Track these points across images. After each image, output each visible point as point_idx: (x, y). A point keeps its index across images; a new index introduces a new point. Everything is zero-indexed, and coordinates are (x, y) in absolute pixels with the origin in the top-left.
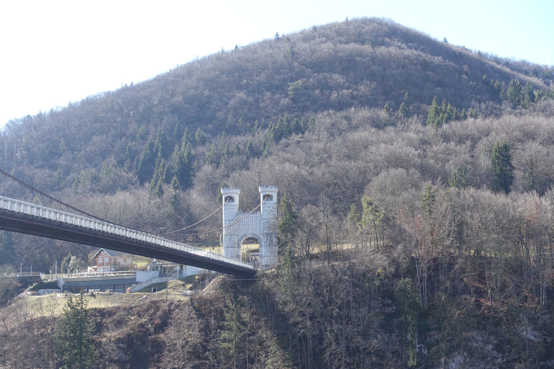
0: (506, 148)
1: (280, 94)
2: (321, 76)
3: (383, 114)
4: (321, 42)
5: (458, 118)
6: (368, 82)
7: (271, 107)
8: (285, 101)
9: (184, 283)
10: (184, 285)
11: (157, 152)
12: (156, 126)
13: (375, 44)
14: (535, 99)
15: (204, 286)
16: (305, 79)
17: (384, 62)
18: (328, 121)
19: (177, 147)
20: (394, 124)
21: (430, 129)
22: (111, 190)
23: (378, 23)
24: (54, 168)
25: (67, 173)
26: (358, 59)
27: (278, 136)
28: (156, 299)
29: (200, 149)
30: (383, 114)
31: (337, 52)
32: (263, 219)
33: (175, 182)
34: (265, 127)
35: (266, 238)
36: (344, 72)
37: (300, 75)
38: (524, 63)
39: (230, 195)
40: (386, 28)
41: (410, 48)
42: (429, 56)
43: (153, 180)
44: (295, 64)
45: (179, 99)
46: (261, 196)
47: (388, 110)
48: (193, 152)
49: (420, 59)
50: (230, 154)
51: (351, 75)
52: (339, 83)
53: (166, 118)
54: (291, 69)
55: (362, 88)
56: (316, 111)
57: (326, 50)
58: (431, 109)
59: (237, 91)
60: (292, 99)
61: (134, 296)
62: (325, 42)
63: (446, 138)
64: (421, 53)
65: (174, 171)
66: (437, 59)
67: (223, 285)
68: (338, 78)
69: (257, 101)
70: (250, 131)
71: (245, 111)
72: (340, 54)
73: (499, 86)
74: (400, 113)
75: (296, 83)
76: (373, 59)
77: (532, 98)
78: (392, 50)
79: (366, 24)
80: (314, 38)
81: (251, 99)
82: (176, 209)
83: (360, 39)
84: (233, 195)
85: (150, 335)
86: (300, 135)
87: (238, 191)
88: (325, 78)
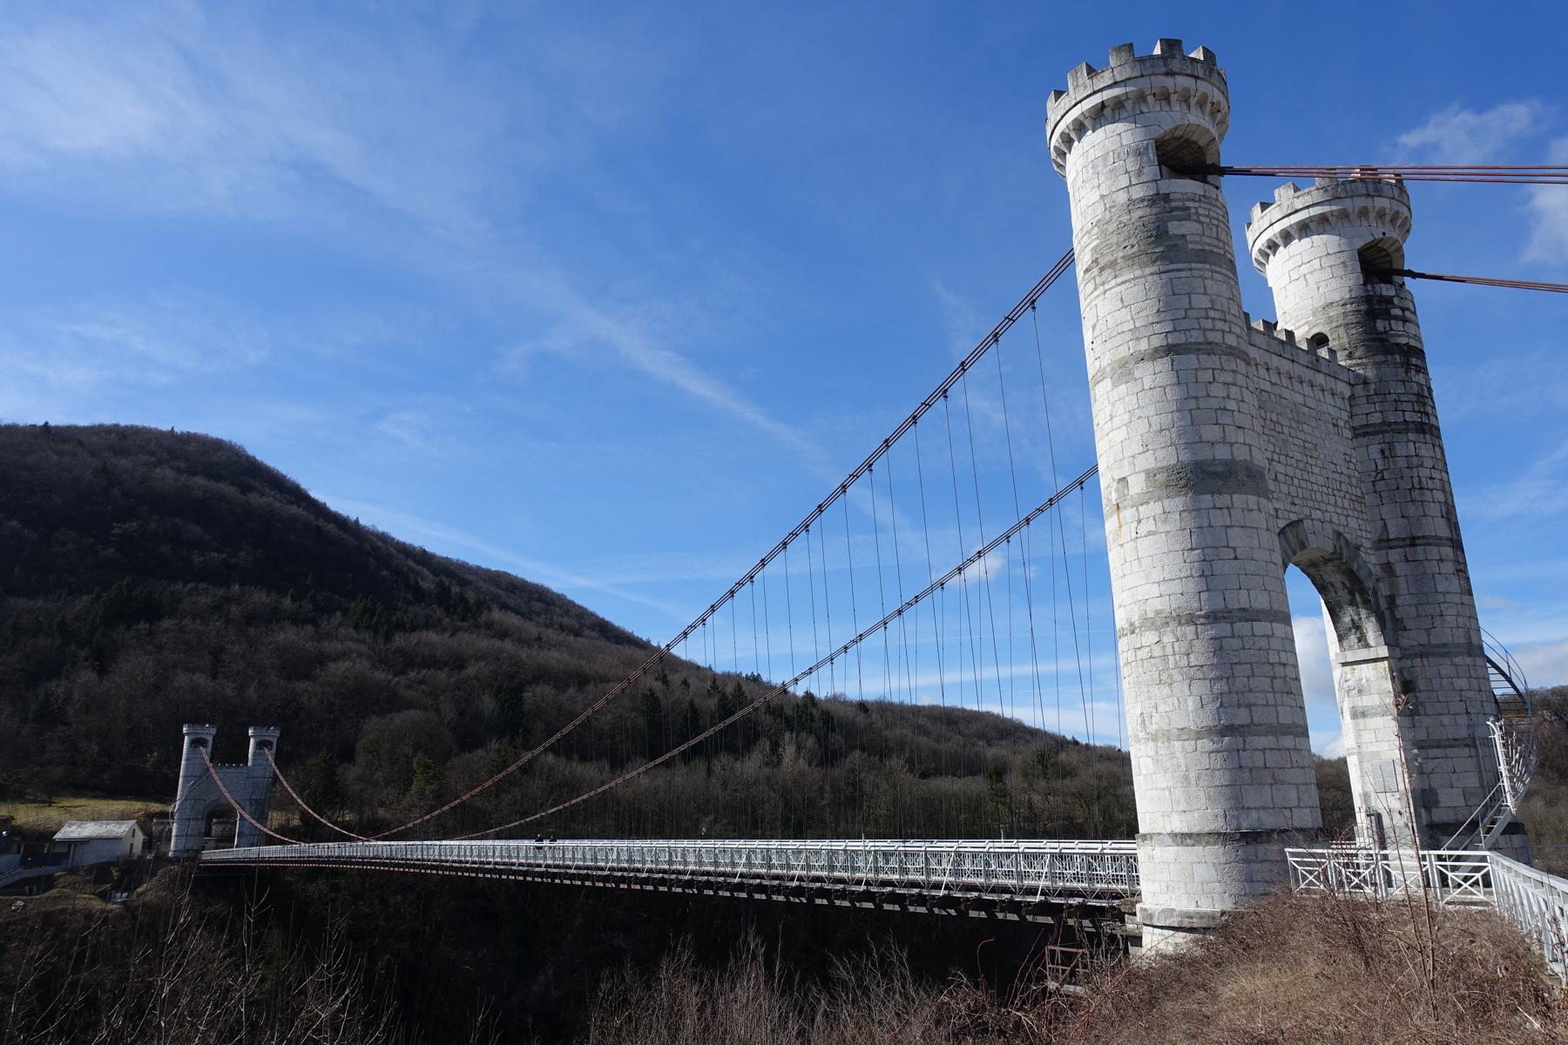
5: (400, 627)
8: (110, 552)
13: (245, 489)
20: (314, 622)
32: (254, 778)
35: (254, 808)
39: (203, 736)
42: (321, 520)
47: (294, 599)
63: (407, 662)
68: (196, 530)
75: (127, 526)
78: (277, 505)
83: (212, 472)
87: (214, 731)
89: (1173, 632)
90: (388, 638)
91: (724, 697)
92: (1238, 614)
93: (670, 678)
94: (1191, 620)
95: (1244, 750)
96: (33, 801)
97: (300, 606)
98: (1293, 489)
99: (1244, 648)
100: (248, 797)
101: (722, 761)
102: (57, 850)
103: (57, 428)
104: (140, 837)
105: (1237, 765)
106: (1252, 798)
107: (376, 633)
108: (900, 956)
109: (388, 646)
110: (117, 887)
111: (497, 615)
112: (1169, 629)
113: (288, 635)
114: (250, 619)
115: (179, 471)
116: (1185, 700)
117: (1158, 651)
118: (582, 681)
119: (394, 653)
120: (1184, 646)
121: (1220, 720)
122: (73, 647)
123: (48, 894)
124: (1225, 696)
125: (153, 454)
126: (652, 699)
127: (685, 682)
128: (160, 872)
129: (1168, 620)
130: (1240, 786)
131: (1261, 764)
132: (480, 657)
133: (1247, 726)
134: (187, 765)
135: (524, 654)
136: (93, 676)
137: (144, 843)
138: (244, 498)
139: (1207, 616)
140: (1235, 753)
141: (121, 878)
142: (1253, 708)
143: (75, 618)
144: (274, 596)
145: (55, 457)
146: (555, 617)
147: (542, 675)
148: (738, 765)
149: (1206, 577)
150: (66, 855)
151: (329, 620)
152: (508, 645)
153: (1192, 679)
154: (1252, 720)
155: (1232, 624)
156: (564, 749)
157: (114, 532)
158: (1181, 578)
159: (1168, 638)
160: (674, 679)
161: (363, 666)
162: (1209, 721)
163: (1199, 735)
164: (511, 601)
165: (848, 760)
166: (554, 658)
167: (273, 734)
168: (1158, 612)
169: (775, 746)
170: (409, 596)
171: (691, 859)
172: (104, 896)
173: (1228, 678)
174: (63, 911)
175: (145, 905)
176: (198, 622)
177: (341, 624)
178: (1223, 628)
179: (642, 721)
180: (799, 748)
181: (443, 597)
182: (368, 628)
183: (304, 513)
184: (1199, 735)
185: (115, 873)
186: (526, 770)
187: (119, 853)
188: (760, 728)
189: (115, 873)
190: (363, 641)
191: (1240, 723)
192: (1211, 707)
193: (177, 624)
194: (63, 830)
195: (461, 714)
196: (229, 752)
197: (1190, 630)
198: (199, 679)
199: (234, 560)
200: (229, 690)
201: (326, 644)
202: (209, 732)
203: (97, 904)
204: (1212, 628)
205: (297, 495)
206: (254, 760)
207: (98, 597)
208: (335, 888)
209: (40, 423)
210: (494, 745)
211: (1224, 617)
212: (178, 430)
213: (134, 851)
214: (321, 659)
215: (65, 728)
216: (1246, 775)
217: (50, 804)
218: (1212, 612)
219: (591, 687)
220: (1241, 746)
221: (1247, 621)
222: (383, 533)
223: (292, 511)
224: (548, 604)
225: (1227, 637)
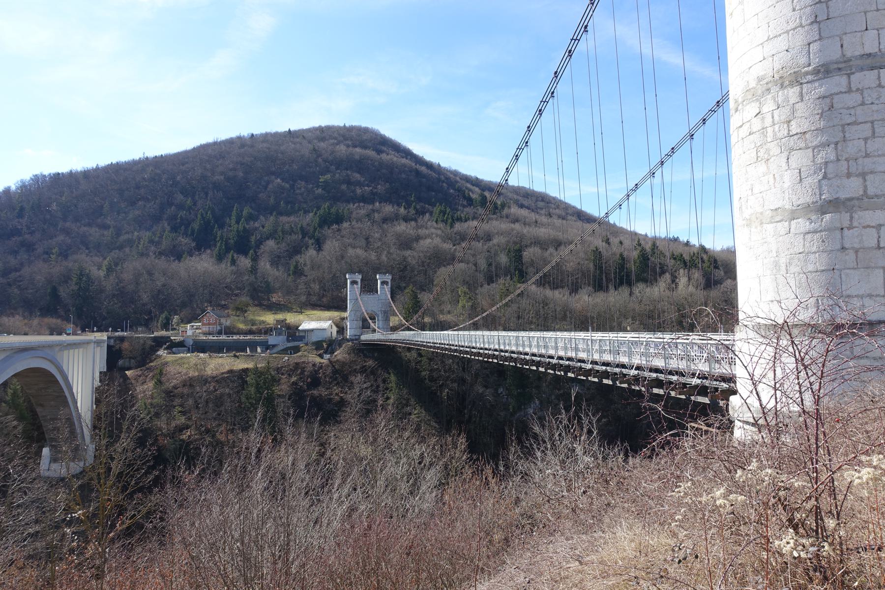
1: (313, 184)
5: (459, 219)
7: (305, 194)
13: (379, 152)
17: (391, 167)
18: (363, 212)
20: (415, 220)
22: (177, 254)
25: (118, 234)
27: (327, 221)
30: (402, 210)
34: (306, 212)
42: (418, 165)
44: (320, 160)
46: (379, 281)
47: (405, 208)
52: (360, 181)
58: (437, 210)
61: (276, 358)
63: (463, 237)
68: (357, 176)
69: (292, 187)
74: (412, 211)
78: (395, 159)
87: (360, 277)
88: (347, 175)
89: (774, 98)
90: (452, 226)
91: (643, 249)
92: (859, 62)
93: (611, 240)
94: (797, 79)
95: (849, 228)
96: (296, 312)
97: (409, 212)
99: (863, 104)
100: (380, 309)
101: (640, 289)
102: (301, 334)
103: (295, 132)
104: (335, 329)
105: (839, 246)
106: (854, 283)
107: (446, 224)
108: (590, 420)
109: (452, 230)
110: (326, 353)
111: (514, 210)
112: (770, 96)
113: (401, 227)
114: (385, 220)
115: (348, 146)
116: (782, 176)
117: (757, 125)
118: (558, 244)
119: (456, 234)
120: (785, 113)
121: (821, 195)
122: (307, 239)
123: (297, 354)
124: (830, 166)
125: (335, 138)
126: (597, 253)
127: (621, 243)
128: (344, 346)
129: (770, 85)
130: (840, 270)
131: (874, 243)
132: (501, 233)
133: (858, 199)
134: (350, 294)
135: (525, 231)
136: (315, 252)
137: (337, 332)
138: (379, 157)
139: (816, 72)
140: (838, 233)
141: (328, 348)
142: (869, 177)
143: (308, 225)
144: (396, 207)
145: (293, 145)
146: (551, 210)
147: (538, 242)
148: (648, 290)
149: (819, 23)
150: (304, 337)
151: (423, 218)
152: (517, 226)
153: (792, 149)
154: (865, 191)
155: (849, 75)
156: (543, 282)
157: (320, 180)
158: (787, 32)
159: (769, 106)
160: (614, 241)
161: (437, 241)
162: (806, 197)
163: (793, 215)
164: (526, 203)
165: (722, 286)
166: (542, 232)
167: (388, 278)
168: (760, 79)
169: (674, 279)
170: (465, 203)
171: (513, 342)
172: (321, 356)
173: (836, 144)
174: (304, 362)
175: (337, 360)
176: (359, 222)
177: (429, 220)
178: (839, 82)
179: (591, 265)
180: (689, 279)
181: (483, 201)
182: (443, 221)
183: (410, 162)
184: (793, 215)
185: (325, 346)
186: (521, 295)
187: (326, 336)
188: (665, 268)
189: (325, 346)
190: (440, 229)
191: (848, 196)
192: (811, 181)
193: (350, 225)
194: (302, 325)
195: (490, 265)
196: (369, 287)
197: (792, 93)
198: (359, 252)
199: (376, 190)
200: (373, 256)
201: (420, 230)
202: (358, 277)
203: (318, 360)
204: (821, 86)
205: (407, 153)
206: (380, 291)
207: (316, 214)
208: (420, 355)
210: (501, 281)
211: (840, 69)
212: (347, 125)
213: (333, 335)
214: (418, 238)
215: (304, 278)
216: (850, 257)
217: (301, 313)
218: (822, 66)
219: (562, 247)
220: (846, 224)
221: (872, 68)
222: (455, 171)
223: (403, 162)
225: (841, 92)
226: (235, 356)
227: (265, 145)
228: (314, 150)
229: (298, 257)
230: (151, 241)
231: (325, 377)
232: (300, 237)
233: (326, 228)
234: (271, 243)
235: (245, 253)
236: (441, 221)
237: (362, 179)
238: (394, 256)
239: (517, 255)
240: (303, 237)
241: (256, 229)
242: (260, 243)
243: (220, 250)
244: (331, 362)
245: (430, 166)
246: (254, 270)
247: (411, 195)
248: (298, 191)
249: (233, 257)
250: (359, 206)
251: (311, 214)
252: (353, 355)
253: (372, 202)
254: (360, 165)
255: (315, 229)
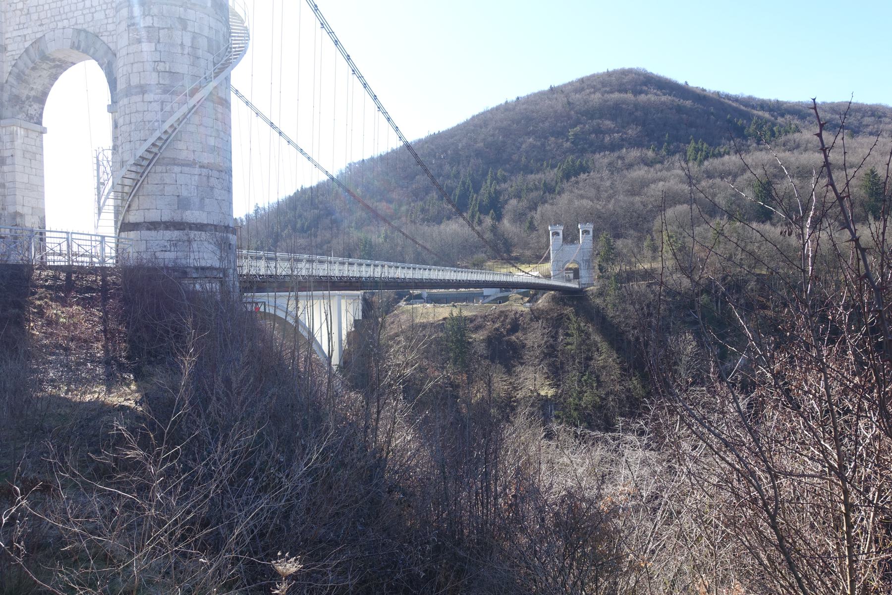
0: (769, 183)
1: (562, 139)
2: (595, 122)
3: (650, 154)
4: (591, 93)
5: (715, 156)
6: (635, 127)
9: (521, 296)
10: (522, 299)
11: (468, 188)
12: (464, 167)
13: (636, 93)
14: (776, 135)
15: (537, 300)
16: (582, 126)
18: (606, 161)
19: (484, 183)
20: (662, 162)
21: (694, 167)
23: (635, 74)
24: (390, 201)
26: (624, 106)
27: (567, 176)
28: (504, 309)
29: (503, 185)
31: (606, 101)
33: (492, 214)
34: (553, 167)
36: (613, 118)
37: (578, 122)
38: (750, 98)
40: (642, 77)
41: (664, 94)
42: (682, 100)
43: (470, 212)
44: (573, 113)
45: (480, 145)
46: (581, 231)
47: (654, 150)
48: (498, 188)
49: (675, 104)
50: (530, 190)
51: (619, 120)
53: (472, 161)
54: (569, 118)
55: (630, 132)
56: (594, 152)
57: (597, 100)
58: (690, 148)
59: (526, 137)
60: (572, 143)
61: (486, 306)
62: (594, 93)
63: (710, 175)
64: (675, 98)
65: (484, 203)
66: (688, 103)
67: (554, 298)
68: (608, 124)
70: (541, 169)
71: (535, 153)
72: (608, 103)
73: (742, 124)
74: (663, 152)
76: (636, 106)
77: (773, 134)
78: (652, 98)
79: (626, 75)
80: (583, 89)
81: (539, 143)
82: (495, 235)
83: (622, 89)
84: (559, 231)
85: (504, 336)
86: (587, 174)
87: (562, 228)
90: (701, 163)
98: (43, 15)
113: (640, 172)
114: (630, 166)
125: (594, 87)
144: (645, 151)
167: (590, 227)
175: (537, 309)
196: (570, 237)
202: (560, 229)
209: (546, 88)
212: (610, 70)
224: (880, 117)
226: (454, 306)
227: (524, 106)
228: (569, 103)
229: (533, 213)
230: (423, 210)
231: (524, 324)
232: (542, 193)
233: (565, 181)
234: (513, 202)
235: (487, 213)
236: (693, 159)
237: (613, 126)
238: (622, 204)
239: (766, 189)
240: (544, 193)
241: (506, 189)
242: (506, 202)
243: (473, 212)
244: (531, 310)
245: (700, 97)
246: (494, 229)
247: (664, 135)
248: (548, 148)
249: (479, 218)
250: (605, 156)
251: (556, 169)
252: (551, 304)
253: (620, 147)
254: (615, 111)
255: (557, 183)
